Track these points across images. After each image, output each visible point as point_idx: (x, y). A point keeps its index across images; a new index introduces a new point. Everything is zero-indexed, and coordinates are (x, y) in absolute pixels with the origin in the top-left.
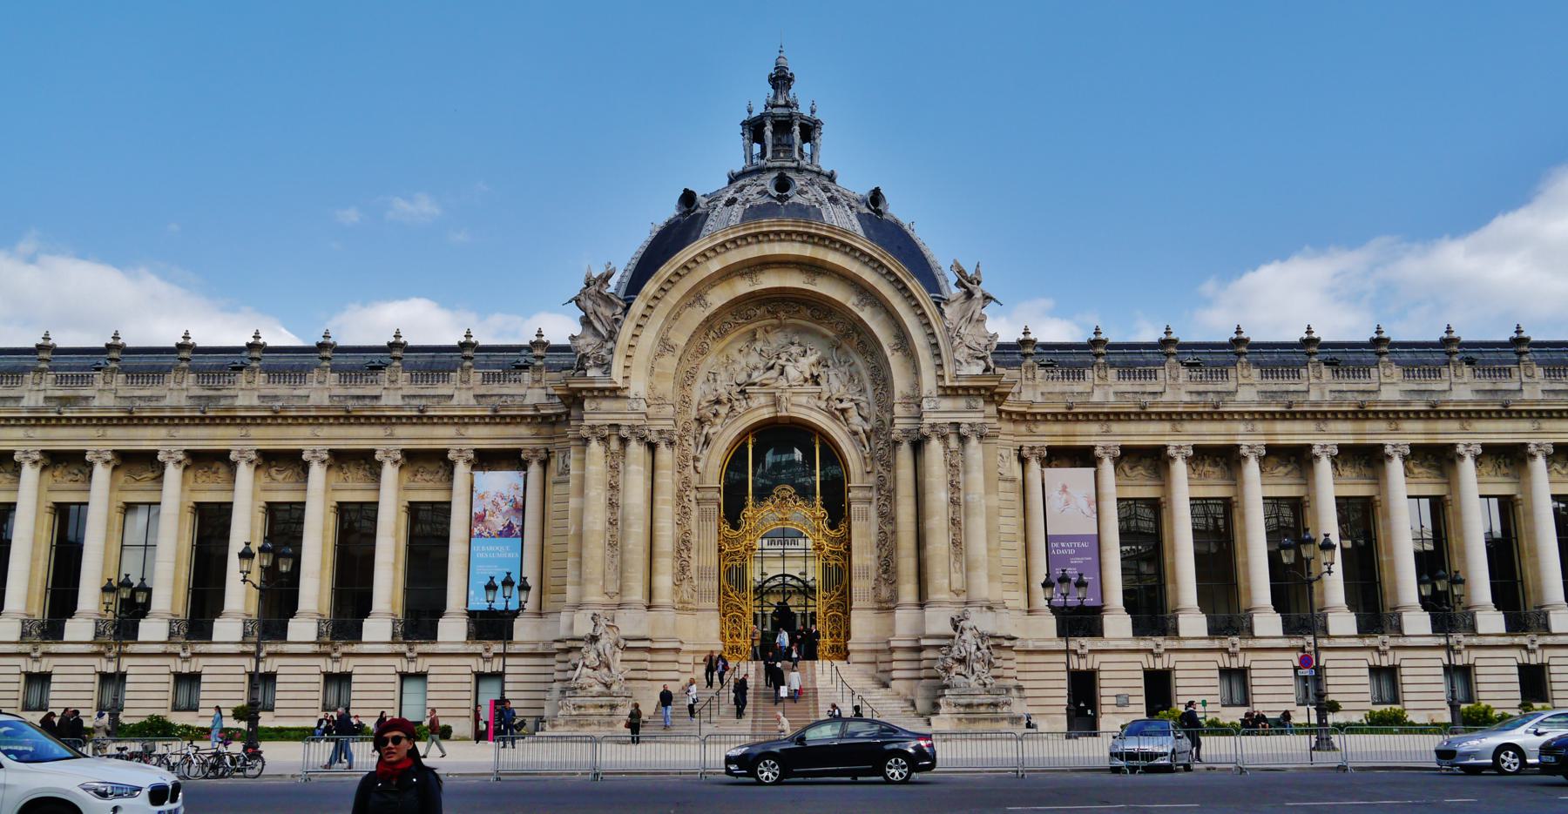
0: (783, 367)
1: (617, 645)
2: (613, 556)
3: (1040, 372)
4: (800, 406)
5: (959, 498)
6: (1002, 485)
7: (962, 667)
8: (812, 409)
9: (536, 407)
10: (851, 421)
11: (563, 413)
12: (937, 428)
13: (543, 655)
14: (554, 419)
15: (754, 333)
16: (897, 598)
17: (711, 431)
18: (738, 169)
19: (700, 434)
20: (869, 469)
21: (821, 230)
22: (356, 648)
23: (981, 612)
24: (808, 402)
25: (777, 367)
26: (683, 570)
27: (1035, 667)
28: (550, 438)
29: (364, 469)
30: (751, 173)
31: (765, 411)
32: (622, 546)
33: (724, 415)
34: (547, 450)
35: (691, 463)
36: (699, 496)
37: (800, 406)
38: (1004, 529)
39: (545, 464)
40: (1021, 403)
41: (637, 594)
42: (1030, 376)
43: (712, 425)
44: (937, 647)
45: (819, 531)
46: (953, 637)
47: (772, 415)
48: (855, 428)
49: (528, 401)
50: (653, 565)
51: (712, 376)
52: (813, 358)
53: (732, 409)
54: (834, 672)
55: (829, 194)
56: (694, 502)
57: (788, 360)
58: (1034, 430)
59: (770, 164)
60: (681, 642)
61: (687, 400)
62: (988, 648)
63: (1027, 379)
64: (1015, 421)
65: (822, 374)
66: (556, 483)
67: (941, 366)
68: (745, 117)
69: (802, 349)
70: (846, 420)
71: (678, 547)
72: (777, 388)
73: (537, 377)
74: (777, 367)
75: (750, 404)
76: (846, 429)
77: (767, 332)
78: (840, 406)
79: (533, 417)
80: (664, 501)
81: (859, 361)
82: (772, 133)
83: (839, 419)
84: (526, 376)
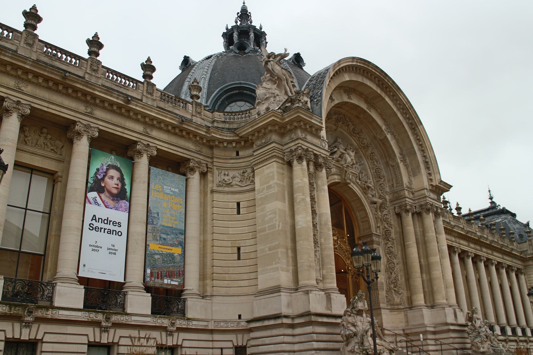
12: (424, 207)
13: (212, 331)
20: (379, 225)
21: (389, 82)
22: (50, 314)
29: (46, 138)
31: (336, 177)
32: (321, 244)
34: (207, 165)
39: (203, 175)
45: (348, 259)
66: (212, 192)
67: (430, 174)
72: (342, 165)
74: (339, 153)
79: (202, 137)
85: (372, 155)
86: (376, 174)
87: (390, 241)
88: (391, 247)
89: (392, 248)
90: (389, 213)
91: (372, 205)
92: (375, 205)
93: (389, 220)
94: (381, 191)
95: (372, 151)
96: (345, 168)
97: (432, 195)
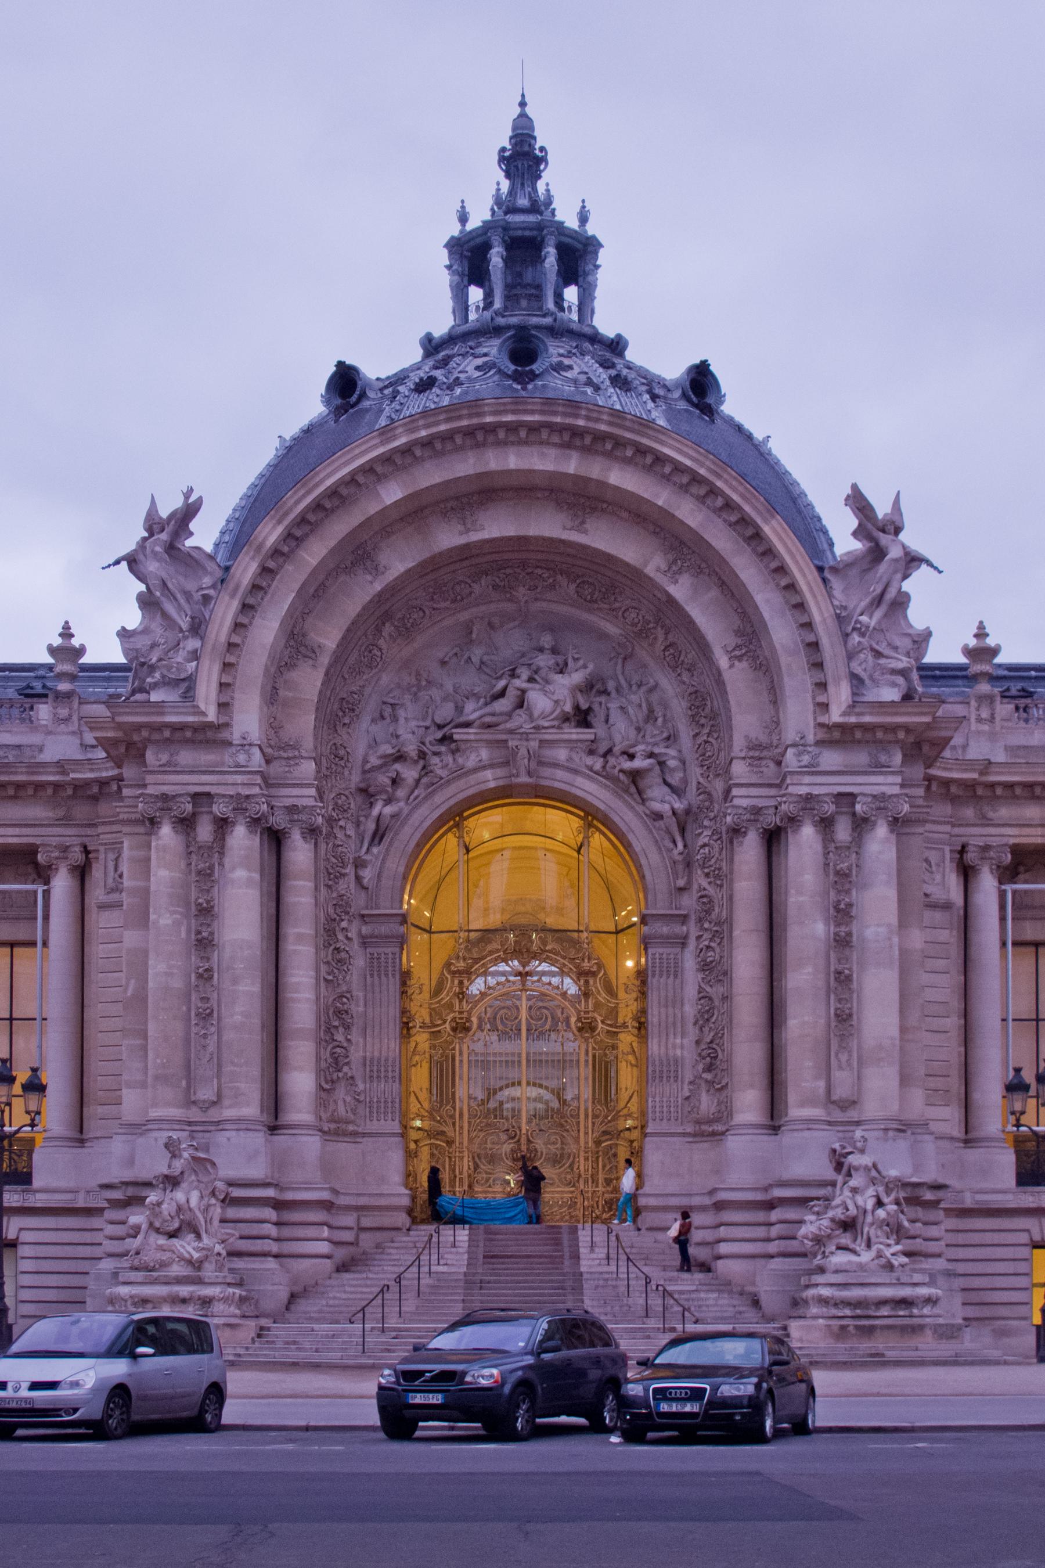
0: (523, 692)
1: (213, 1194)
2: (205, 1036)
3: (1004, 709)
4: (556, 765)
5: (849, 934)
6: (929, 915)
7: (848, 1235)
8: (575, 772)
9: (61, 766)
10: (649, 793)
11: (113, 778)
14: (95, 789)
15: (468, 628)
16: (730, 1115)
17: (388, 810)
18: (442, 324)
19: (367, 817)
20: (681, 883)
23: (886, 1140)
24: (570, 759)
25: (512, 693)
26: (337, 1062)
27: (976, 1238)
28: (90, 825)
30: (465, 336)
31: (489, 774)
32: (219, 1019)
33: (410, 781)
35: (349, 870)
36: (365, 930)
37: (556, 765)
38: (930, 994)
40: (969, 765)
41: (252, 1109)
42: (985, 714)
43: (388, 802)
44: (803, 1202)
46: (833, 1184)
47: (501, 783)
48: (656, 806)
49: (47, 756)
50: (281, 1054)
51: (388, 710)
52: (577, 677)
53: (426, 770)
54: (613, 1243)
55: (613, 372)
56: (356, 944)
57: (531, 680)
58: (991, 814)
59: (501, 321)
60: (335, 1192)
61: (342, 752)
62: (897, 1203)
63: (979, 720)
64: (954, 800)
65: (596, 707)
68: (455, 230)
69: (560, 659)
70: (640, 792)
71: (328, 1022)
72: (511, 732)
73: (64, 712)
74: (512, 694)
75: (460, 761)
76: (640, 809)
77: (491, 625)
78: (628, 765)
80: (300, 937)
81: (668, 684)
82: (506, 261)
83: (626, 791)
84: (44, 711)
85: (667, 653)
86: (690, 713)
87: (706, 930)
88: (708, 947)
89: (714, 951)
90: (715, 837)
91: (657, 824)
92: (661, 822)
93: (713, 861)
94: (702, 766)
95: (666, 639)
96: (511, 744)
97: (831, 759)
